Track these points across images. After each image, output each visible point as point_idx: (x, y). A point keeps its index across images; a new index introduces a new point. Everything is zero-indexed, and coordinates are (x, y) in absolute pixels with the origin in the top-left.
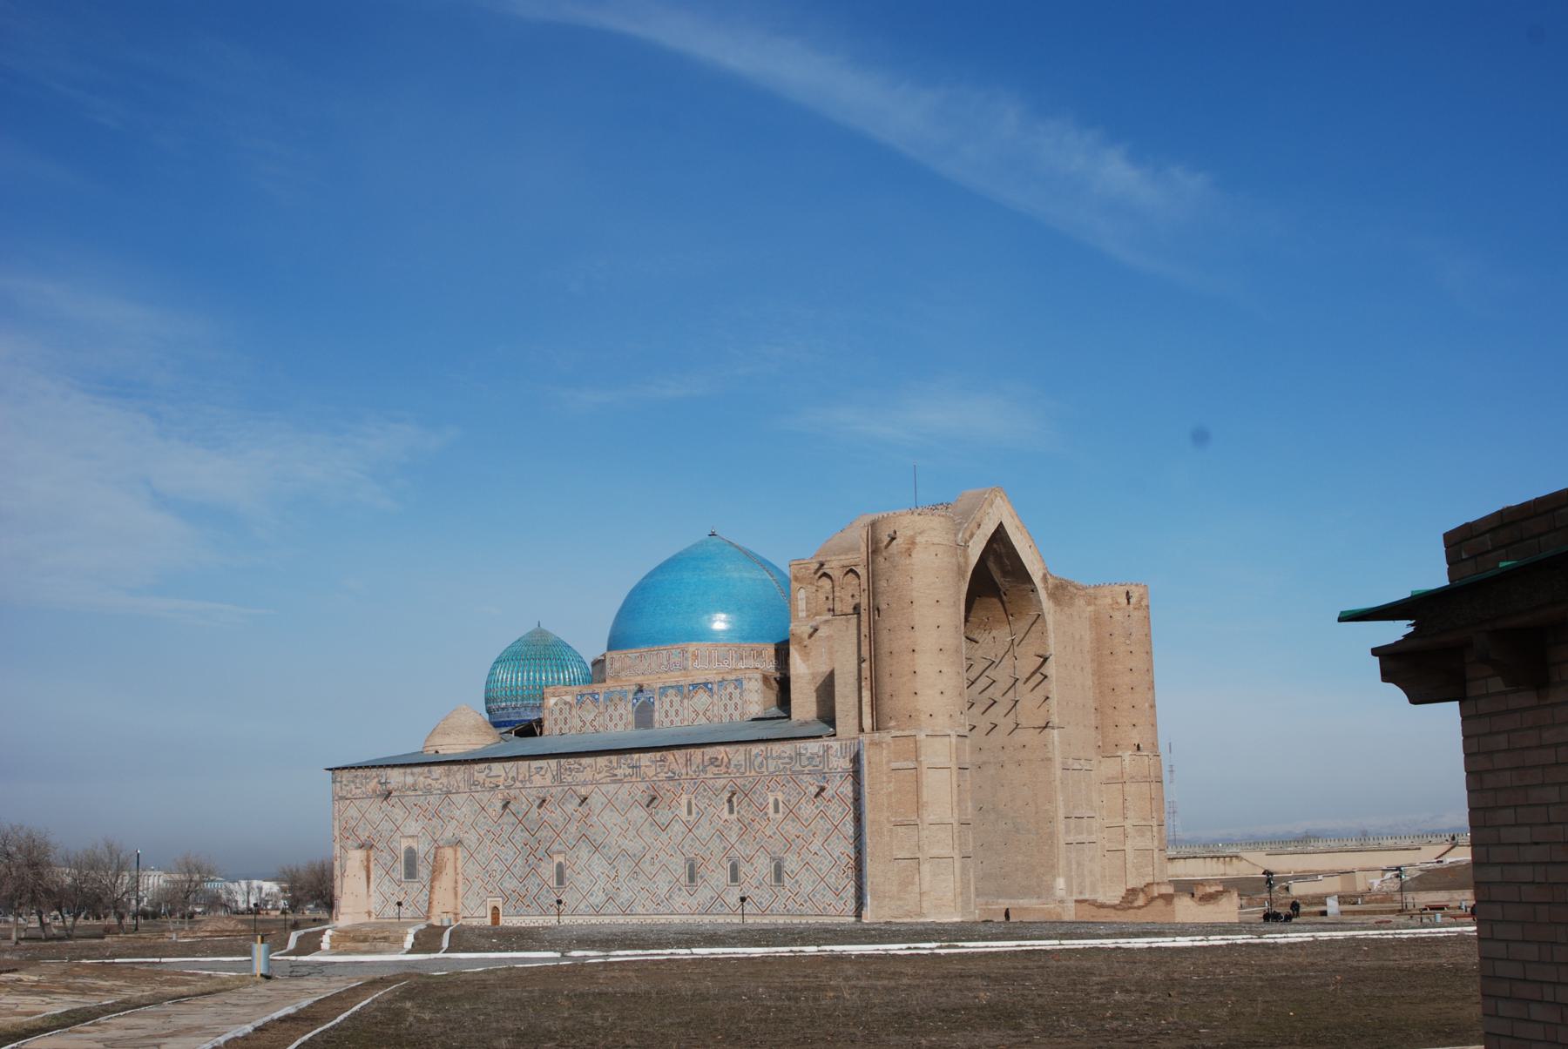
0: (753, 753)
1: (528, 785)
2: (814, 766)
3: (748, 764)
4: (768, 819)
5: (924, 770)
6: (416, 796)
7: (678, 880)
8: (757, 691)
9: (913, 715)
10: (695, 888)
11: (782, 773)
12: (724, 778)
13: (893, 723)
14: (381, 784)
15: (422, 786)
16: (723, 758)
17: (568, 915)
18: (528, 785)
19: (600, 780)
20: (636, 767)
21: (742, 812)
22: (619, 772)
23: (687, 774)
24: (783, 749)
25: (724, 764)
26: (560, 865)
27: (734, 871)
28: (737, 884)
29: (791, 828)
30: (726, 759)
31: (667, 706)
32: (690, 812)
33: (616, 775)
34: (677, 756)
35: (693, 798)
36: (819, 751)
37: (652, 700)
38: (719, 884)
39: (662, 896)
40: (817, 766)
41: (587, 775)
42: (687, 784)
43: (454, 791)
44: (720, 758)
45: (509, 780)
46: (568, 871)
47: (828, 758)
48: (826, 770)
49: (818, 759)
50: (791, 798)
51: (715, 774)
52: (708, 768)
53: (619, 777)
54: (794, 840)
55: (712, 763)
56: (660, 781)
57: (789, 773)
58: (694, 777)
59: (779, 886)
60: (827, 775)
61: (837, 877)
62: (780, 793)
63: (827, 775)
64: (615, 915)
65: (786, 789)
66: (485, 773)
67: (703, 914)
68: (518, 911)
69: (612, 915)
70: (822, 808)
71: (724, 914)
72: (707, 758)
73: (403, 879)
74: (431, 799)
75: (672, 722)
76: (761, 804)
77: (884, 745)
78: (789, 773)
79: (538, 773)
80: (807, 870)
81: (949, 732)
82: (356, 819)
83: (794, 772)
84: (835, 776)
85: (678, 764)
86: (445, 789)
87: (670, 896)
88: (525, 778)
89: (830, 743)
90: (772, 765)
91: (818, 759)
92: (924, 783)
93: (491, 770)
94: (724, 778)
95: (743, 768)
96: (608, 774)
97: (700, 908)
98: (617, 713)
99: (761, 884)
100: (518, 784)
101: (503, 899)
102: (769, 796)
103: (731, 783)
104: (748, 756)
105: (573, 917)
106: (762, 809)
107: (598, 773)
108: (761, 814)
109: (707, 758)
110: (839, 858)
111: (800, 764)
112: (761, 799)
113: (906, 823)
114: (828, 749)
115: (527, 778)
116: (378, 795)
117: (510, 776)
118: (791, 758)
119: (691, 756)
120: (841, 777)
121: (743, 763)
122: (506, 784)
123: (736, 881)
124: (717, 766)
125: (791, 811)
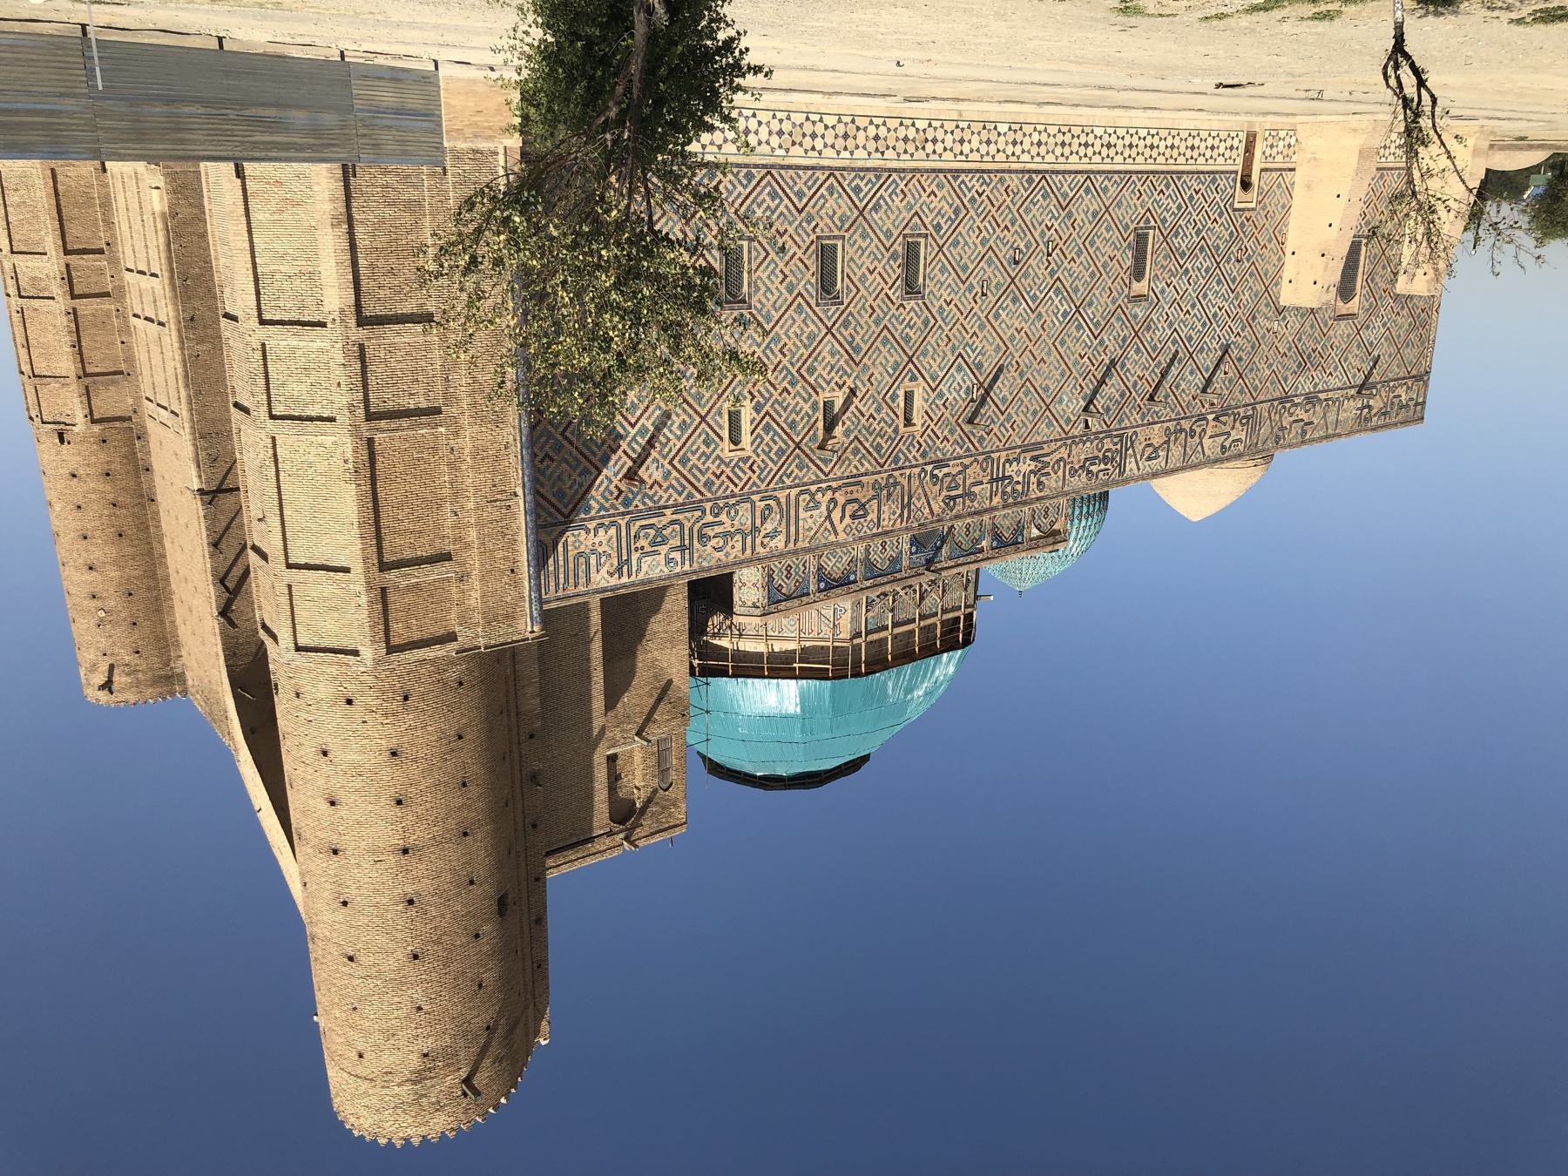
0: (782, 537)
1: (1171, 425)
2: (651, 526)
4: (754, 397)
5: (358, 568)
6: (1326, 391)
7: (941, 248)
8: (744, 584)
9: (396, 705)
10: (905, 232)
11: (721, 503)
12: (842, 478)
13: (452, 675)
14: (1369, 407)
15: (1318, 408)
17: (1137, 172)
19: (1060, 447)
20: (997, 480)
21: (807, 407)
22: (1027, 466)
23: (910, 476)
24: (721, 555)
25: (839, 509)
26: (1138, 274)
28: (824, 242)
30: (836, 515)
32: (909, 397)
33: (1034, 459)
34: (927, 510)
35: (902, 429)
39: (972, 212)
40: (643, 527)
42: (910, 457)
43: (1276, 403)
44: (848, 520)
45: (1198, 430)
46: (1129, 263)
49: (643, 542)
50: (703, 448)
52: (872, 493)
53: (1029, 455)
55: (864, 505)
56: (960, 458)
57: (708, 506)
58: (896, 473)
60: (622, 509)
62: (727, 455)
63: (622, 509)
64: (1058, 172)
65: (713, 468)
66: (1231, 439)
67: (895, 170)
68: (1214, 181)
69: (1064, 172)
70: (633, 432)
72: (872, 516)
74: (1308, 387)
76: (767, 429)
77: (477, 618)
81: (301, 659)
82: (1408, 345)
84: (602, 507)
85: (926, 495)
86: (1288, 405)
87: (956, 212)
88: (1176, 439)
90: (744, 517)
91: (643, 542)
92: (356, 531)
93: (1223, 447)
94: (842, 478)
95: (802, 505)
96: (1046, 459)
101: (1232, 205)
102: (748, 447)
103: (826, 470)
104: (793, 529)
106: (765, 420)
107: (1061, 459)
108: (767, 407)
109: (872, 516)
111: (682, 526)
112: (767, 438)
113: (405, 423)
114: (619, 570)
115: (1173, 438)
116: (1375, 387)
117: (1196, 438)
119: (901, 515)
121: (802, 515)
122: (1204, 422)
124: (856, 500)
125: (703, 419)
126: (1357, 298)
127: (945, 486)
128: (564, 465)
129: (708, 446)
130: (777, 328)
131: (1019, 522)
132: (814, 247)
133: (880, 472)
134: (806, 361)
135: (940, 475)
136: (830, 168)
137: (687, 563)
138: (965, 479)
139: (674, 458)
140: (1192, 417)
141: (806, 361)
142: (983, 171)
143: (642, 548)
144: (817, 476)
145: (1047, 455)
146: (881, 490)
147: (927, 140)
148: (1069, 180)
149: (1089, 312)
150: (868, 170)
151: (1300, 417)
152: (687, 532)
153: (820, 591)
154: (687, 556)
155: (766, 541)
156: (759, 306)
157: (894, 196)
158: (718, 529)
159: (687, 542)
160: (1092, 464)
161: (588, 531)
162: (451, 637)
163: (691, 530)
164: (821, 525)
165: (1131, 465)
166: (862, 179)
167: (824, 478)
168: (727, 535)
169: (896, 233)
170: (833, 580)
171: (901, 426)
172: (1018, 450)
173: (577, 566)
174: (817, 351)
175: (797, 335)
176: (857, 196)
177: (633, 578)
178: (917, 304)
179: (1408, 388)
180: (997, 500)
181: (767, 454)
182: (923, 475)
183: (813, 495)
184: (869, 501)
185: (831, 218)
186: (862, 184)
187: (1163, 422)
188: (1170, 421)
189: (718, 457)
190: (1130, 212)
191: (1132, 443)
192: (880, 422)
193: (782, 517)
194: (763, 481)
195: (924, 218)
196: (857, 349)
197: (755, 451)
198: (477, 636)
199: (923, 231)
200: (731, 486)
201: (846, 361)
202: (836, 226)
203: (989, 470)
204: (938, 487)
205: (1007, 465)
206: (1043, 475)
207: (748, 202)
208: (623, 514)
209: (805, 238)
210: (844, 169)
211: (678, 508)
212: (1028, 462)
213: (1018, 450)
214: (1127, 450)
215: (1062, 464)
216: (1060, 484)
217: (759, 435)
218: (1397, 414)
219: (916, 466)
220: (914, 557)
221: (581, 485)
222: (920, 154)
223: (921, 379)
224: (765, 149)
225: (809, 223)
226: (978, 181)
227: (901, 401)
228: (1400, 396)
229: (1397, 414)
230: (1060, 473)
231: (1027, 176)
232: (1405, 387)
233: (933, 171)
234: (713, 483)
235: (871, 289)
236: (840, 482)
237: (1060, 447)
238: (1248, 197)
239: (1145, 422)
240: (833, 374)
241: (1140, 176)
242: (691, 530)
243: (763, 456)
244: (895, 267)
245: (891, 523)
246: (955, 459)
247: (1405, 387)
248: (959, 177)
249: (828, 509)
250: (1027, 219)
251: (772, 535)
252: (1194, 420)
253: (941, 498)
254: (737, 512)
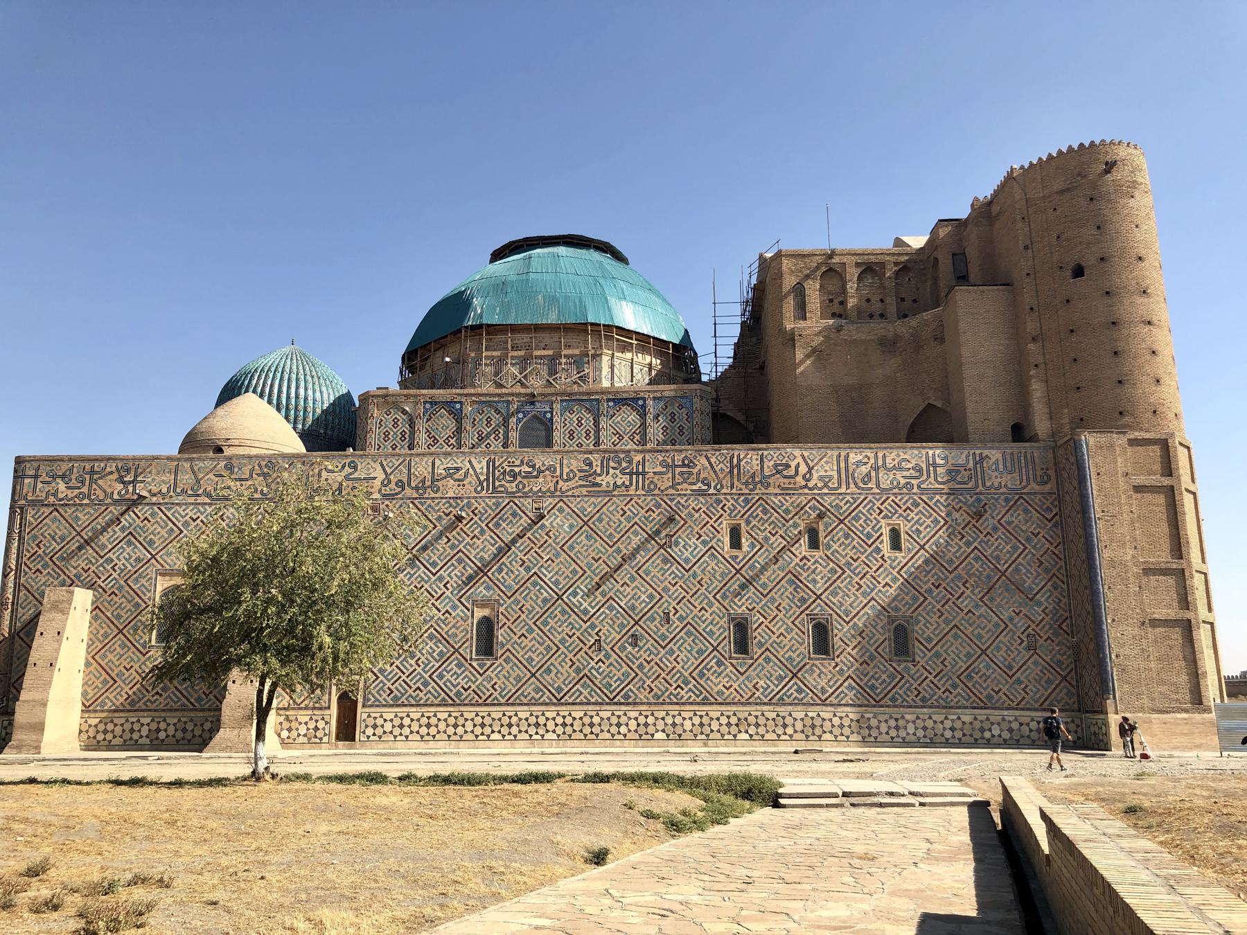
2: (960, 483)
3: (843, 477)
4: (882, 557)
9: (1160, 409)
16: (798, 466)
17: (499, 705)
18: (430, 493)
19: (568, 490)
23: (732, 487)
24: (903, 456)
30: (803, 469)
32: (736, 543)
33: (599, 485)
34: (713, 460)
36: (968, 461)
37: (549, 415)
38: (794, 656)
40: (964, 483)
42: (732, 501)
44: (793, 464)
45: (393, 486)
47: (983, 472)
51: (783, 489)
52: (771, 481)
53: (604, 488)
54: (929, 591)
55: (778, 472)
56: (679, 495)
59: (908, 661)
61: (1009, 649)
65: (912, 515)
66: (344, 473)
67: (765, 704)
69: (588, 704)
71: (804, 704)
72: (769, 464)
73: (153, 643)
78: (915, 490)
79: (451, 476)
80: (956, 637)
83: (923, 491)
84: (997, 500)
85: (715, 472)
88: (423, 481)
89: (986, 452)
90: (886, 480)
93: (355, 468)
95: (835, 480)
96: (581, 483)
97: (758, 694)
99: (872, 658)
100: (408, 492)
104: (843, 465)
105: (510, 708)
106: (870, 541)
107: (567, 481)
109: (769, 464)
110: (1011, 619)
111: (936, 480)
115: (428, 483)
116: (117, 501)
120: (1007, 500)
121: (835, 474)
124: (785, 477)
126: (159, 589)
127: (695, 476)
128: (1024, 528)
129: (917, 530)
130: (865, 601)
131: (428, 420)
132: (837, 653)
133: (763, 494)
134: (838, 578)
135: (700, 484)
136: (826, 705)
137: (930, 455)
138: (673, 478)
139: (944, 525)
140: (402, 499)
141: (838, 578)
142: (677, 704)
143: (965, 470)
144: (823, 499)
145: (581, 486)
146: (761, 481)
147: (737, 725)
148: (582, 697)
149: (545, 594)
150: (790, 704)
151: (238, 483)
152: (932, 475)
153: (644, 399)
154: (931, 459)
155: (866, 460)
156: (882, 617)
157: (765, 686)
158: (905, 473)
159: (931, 469)
160: (529, 473)
161: (1006, 486)
162: (1133, 442)
163: (929, 476)
164: (817, 464)
165: (481, 465)
166: (533, 698)
167: (817, 497)
169: (760, 660)
170: (629, 405)
171: (743, 525)
172: (615, 493)
173: (1013, 465)
174: (828, 584)
175: (848, 595)
176: (799, 686)
177: (972, 452)
178: (733, 609)
179: (55, 495)
180: (639, 457)
181: (867, 519)
182: (719, 487)
183: (826, 486)
184: (773, 475)
185: (822, 672)
186: (795, 694)
187: (442, 498)
188: (433, 498)
189: (909, 521)
190: (500, 673)
191: (481, 483)
192: (766, 529)
193: (853, 475)
194: (870, 501)
195: (734, 671)
196: (791, 582)
197: (879, 522)
198: (1121, 441)
199: (734, 662)
200: (897, 501)
201: (801, 575)
202: (816, 666)
203: (647, 482)
204: (702, 476)
205: (627, 483)
206: (586, 471)
207: (894, 684)
208: (981, 494)
209: (844, 660)
210: (812, 705)
212: (604, 483)
213: (615, 493)
214: (488, 479)
215: (565, 477)
216: (565, 462)
217: (876, 532)
218: (71, 470)
219: (725, 494)
220: (548, 409)
221: (1012, 515)
222: (742, 716)
223: (726, 556)
224: (882, 718)
225: (842, 669)
226: (683, 697)
227: (745, 542)
228: (68, 488)
229: (71, 470)
230: (566, 470)
231: (630, 700)
232: (61, 496)
233: (729, 703)
234: (912, 505)
235: (781, 623)
236: (800, 491)
237: (568, 490)
239: (466, 501)
240: (813, 567)
241: (496, 702)
242: (929, 476)
243: (872, 518)
244: (759, 637)
245: (749, 456)
246: (685, 495)
247: (61, 496)
248: (703, 699)
249: (811, 474)
250: (625, 668)
252: (400, 496)
253: (698, 467)
254: (892, 483)
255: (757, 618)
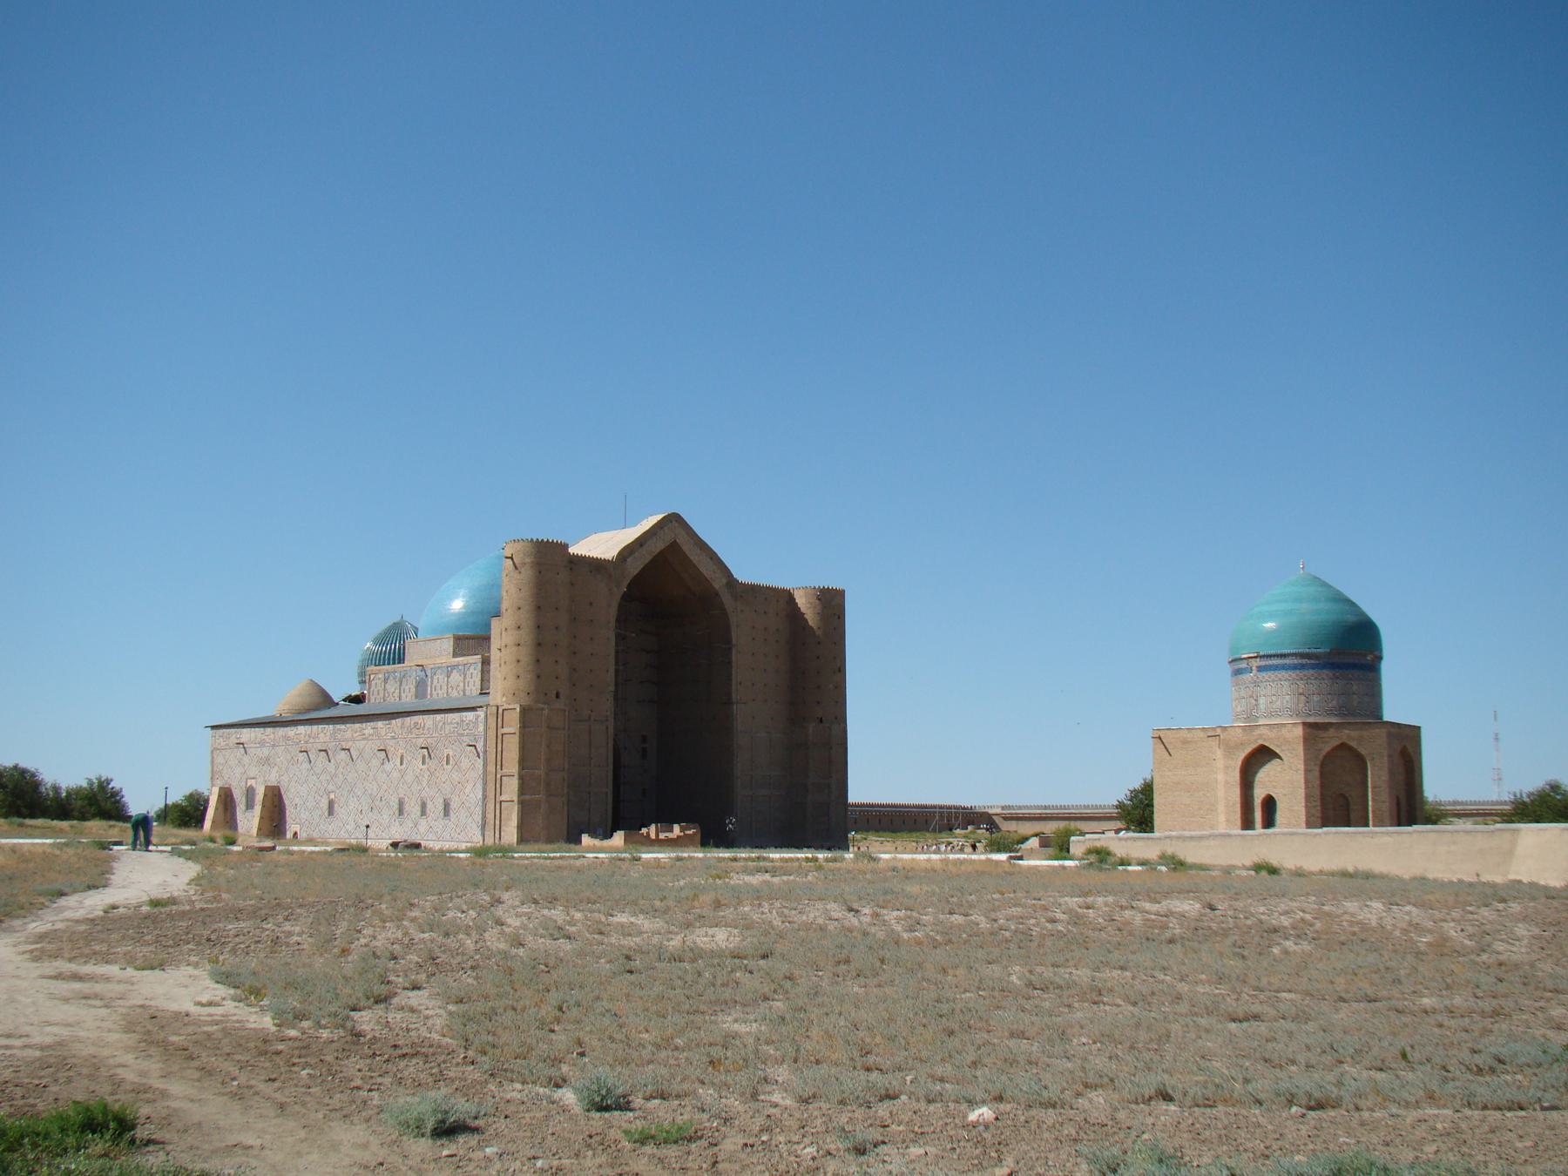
1: (317, 741)
22: (366, 732)
27: (424, 806)
29: (456, 777)
31: (435, 681)
32: (401, 764)
33: (364, 734)
41: (348, 734)
48: (476, 733)
75: (438, 694)
98: (407, 687)
100: (312, 740)
118: (458, 724)
123: (425, 815)
168: (451, 723)
211: (462, 735)
238: (295, 830)
251: (440, 721)
255: (406, 799)
